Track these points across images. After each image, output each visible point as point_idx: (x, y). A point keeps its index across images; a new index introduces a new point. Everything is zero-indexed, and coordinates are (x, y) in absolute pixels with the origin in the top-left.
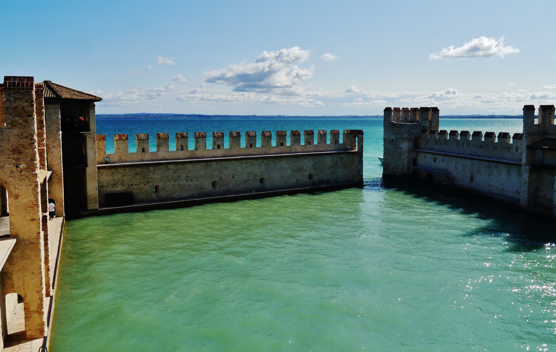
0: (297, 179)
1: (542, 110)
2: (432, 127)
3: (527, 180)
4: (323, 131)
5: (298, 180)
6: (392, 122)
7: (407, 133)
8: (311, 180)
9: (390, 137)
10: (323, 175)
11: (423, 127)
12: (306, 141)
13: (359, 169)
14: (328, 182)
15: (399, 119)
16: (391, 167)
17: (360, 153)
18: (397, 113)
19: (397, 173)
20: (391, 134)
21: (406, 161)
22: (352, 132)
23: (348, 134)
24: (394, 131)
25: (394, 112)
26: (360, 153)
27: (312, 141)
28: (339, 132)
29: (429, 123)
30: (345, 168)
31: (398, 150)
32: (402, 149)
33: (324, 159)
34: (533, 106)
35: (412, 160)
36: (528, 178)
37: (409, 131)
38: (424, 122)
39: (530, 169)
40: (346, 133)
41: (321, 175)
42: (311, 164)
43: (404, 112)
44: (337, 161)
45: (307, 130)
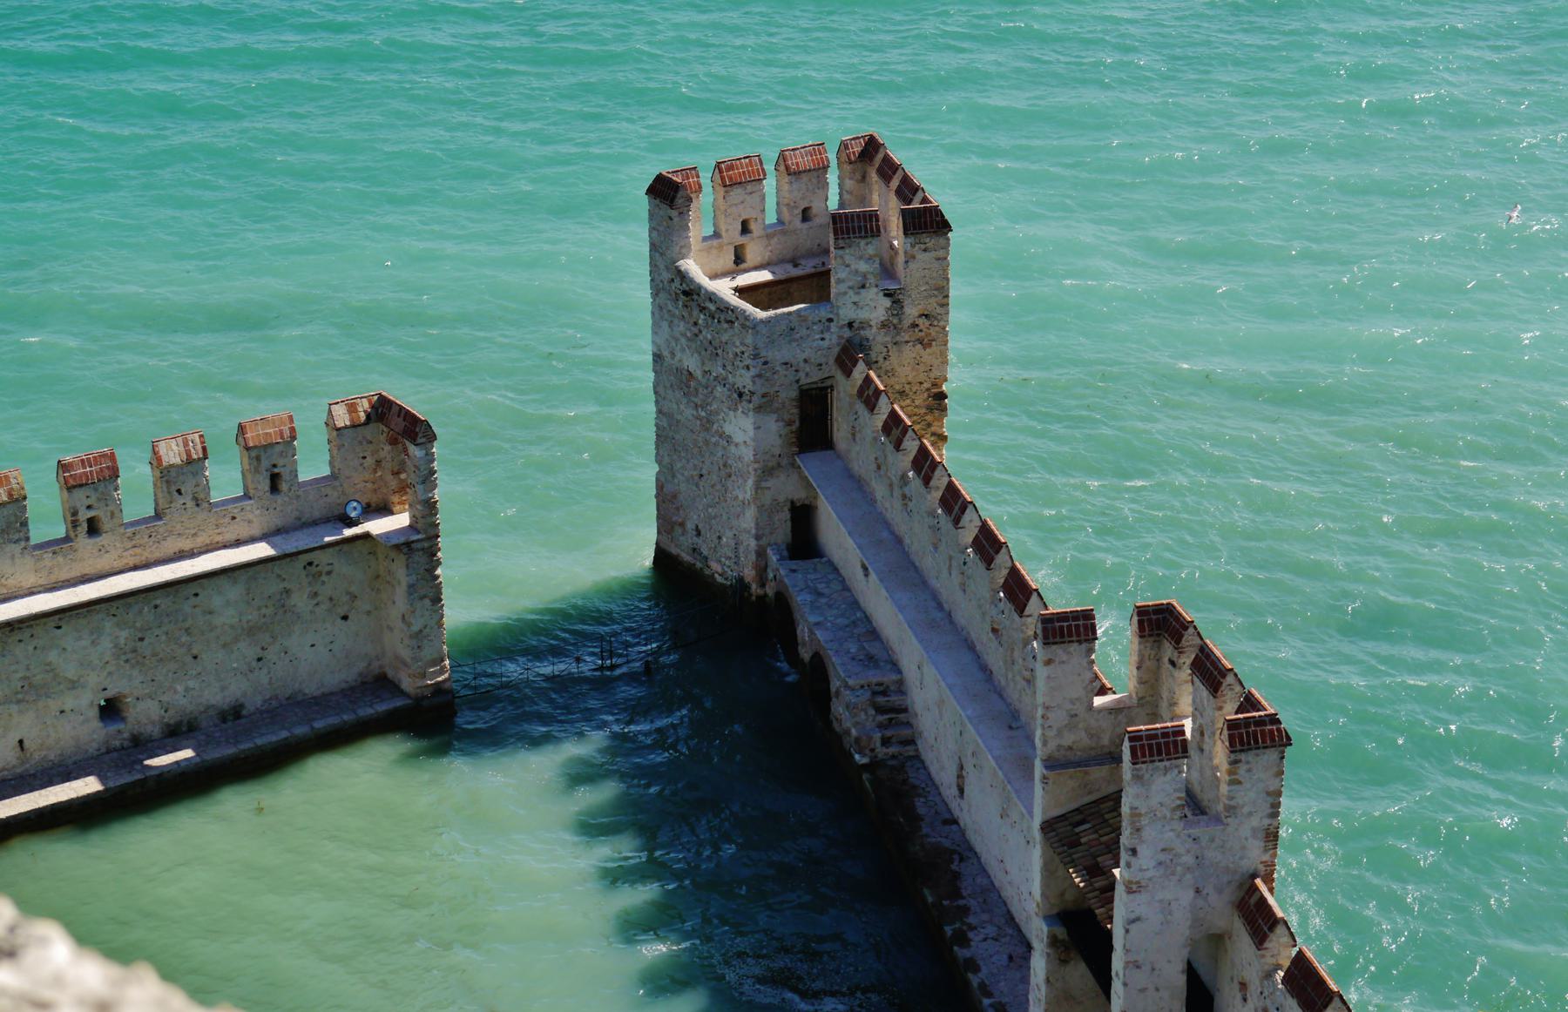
0: (21, 742)
1: (1141, 637)
2: (907, 323)
3: (1043, 988)
4: (186, 444)
5: (27, 744)
6: (683, 276)
7: (748, 368)
8: (113, 728)
9: (679, 355)
10: (191, 684)
11: (850, 325)
12: (70, 518)
13: (415, 628)
14: (233, 713)
15: (753, 226)
16: (690, 526)
17: (419, 545)
18: (737, 193)
19: (715, 566)
20: (683, 341)
21: (748, 520)
22: (383, 409)
23: (354, 426)
24: (695, 330)
25: (721, 190)
26: (419, 545)
27: (112, 514)
28: (293, 430)
29: (887, 302)
30: (345, 618)
31: (714, 440)
32: (733, 448)
33: (193, 600)
34: (1088, 616)
35: (786, 515)
36: (1048, 981)
37: (756, 356)
38: (856, 299)
39: (1054, 941)
40: (342, 418)
41: (180, 688)
42: (106, 644)
43: (787, 179)
44: (287, 591)
45: (68, 458)
